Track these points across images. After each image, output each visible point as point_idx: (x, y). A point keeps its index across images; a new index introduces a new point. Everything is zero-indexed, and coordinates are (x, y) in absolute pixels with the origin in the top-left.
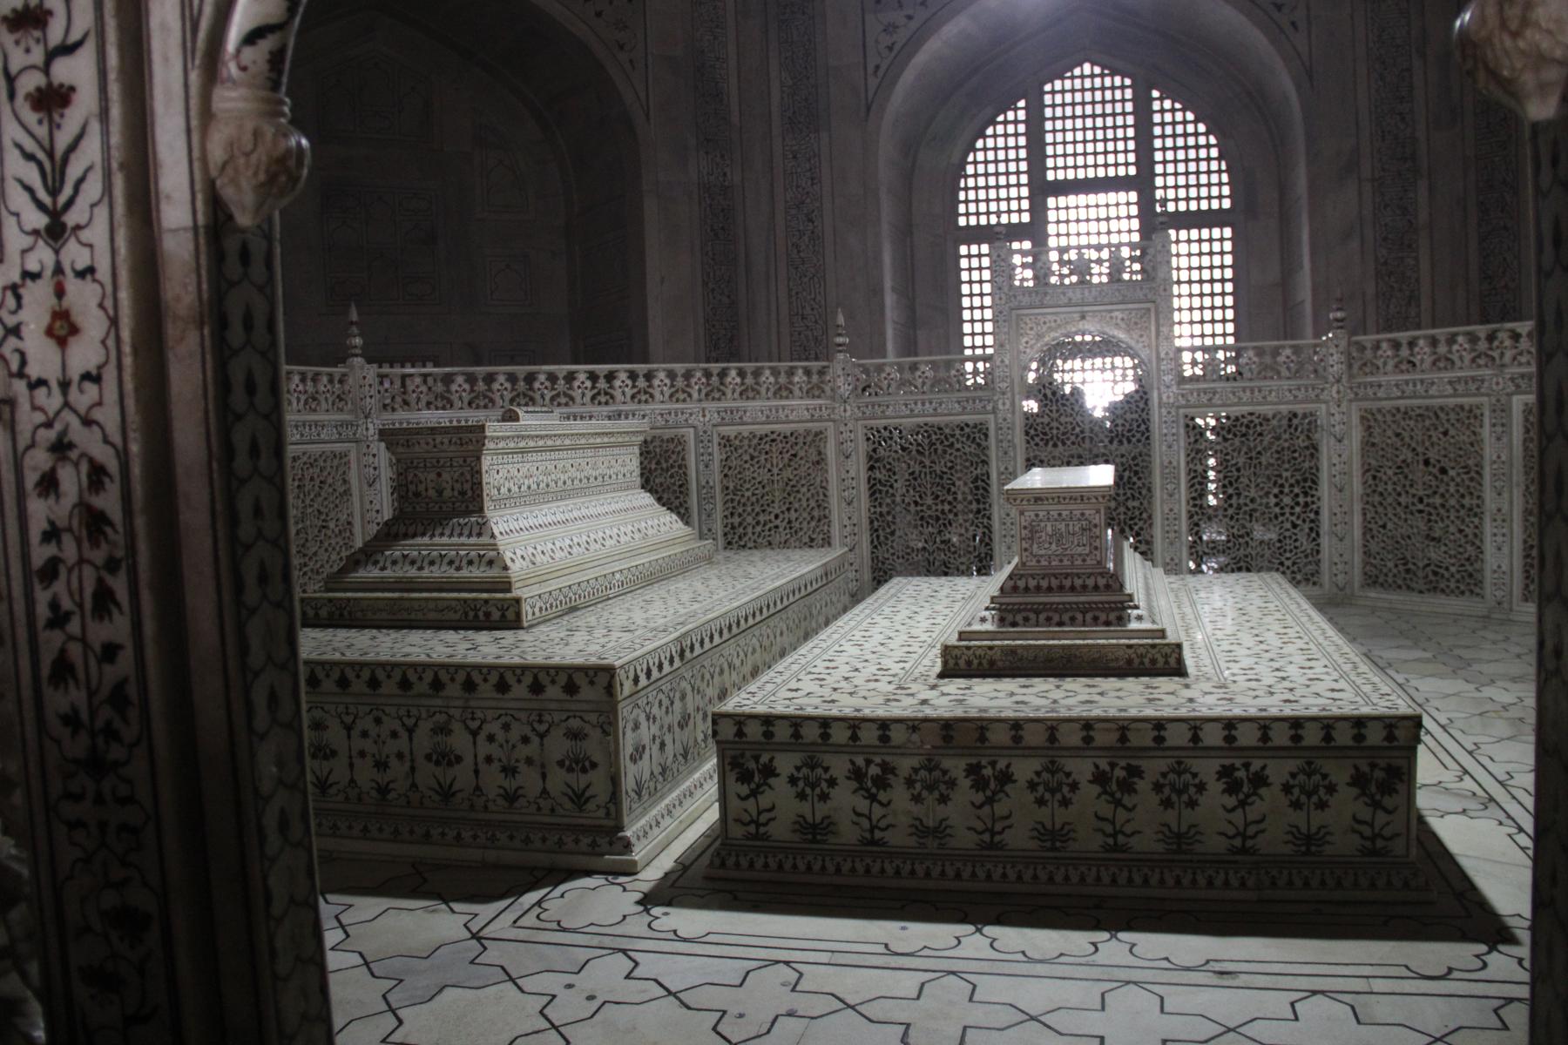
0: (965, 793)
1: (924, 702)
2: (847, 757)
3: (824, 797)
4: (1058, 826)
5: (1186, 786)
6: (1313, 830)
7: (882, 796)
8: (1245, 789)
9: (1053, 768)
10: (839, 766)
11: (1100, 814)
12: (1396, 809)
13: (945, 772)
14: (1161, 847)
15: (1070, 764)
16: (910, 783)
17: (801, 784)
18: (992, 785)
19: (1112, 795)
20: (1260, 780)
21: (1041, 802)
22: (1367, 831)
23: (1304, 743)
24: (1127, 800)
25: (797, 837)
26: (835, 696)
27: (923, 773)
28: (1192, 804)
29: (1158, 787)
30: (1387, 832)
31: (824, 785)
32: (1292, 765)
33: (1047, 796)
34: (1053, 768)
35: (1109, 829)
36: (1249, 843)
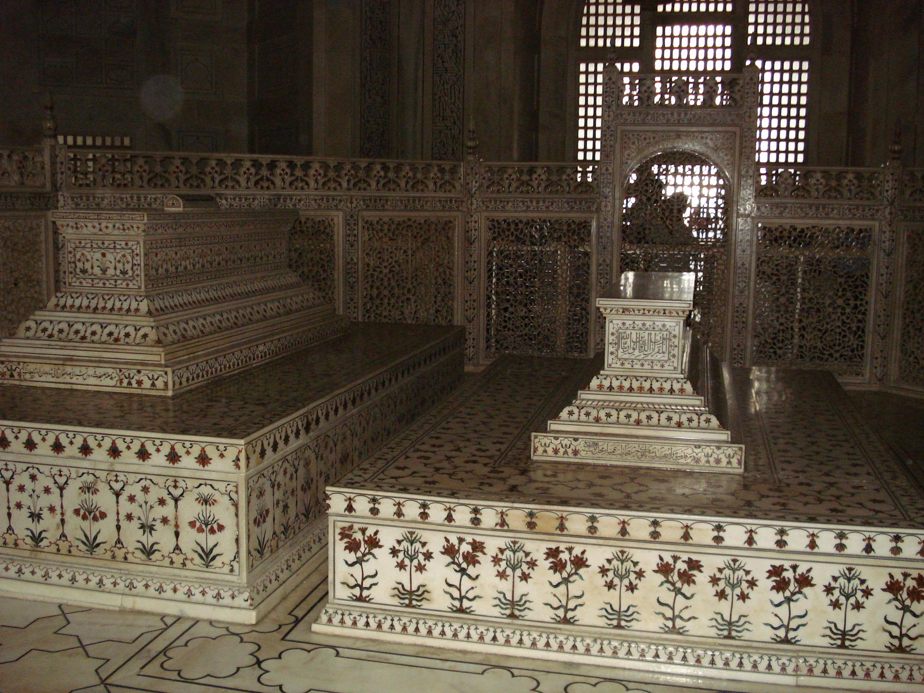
0: (543, 573)
2: (443, 535)
4: (624, 608)
5: (740, 582)
6: (848, 628)
15: (637, 555)
16: (496, 560)
17: (401, 555)
19: (673, 584)
20: (805, 581)
25: (396, 601)
29: (714, 581)
31: (421, 557)
33: (616, 581)
34: (622, 557)
35: (669, 614)
36: (791, 635)
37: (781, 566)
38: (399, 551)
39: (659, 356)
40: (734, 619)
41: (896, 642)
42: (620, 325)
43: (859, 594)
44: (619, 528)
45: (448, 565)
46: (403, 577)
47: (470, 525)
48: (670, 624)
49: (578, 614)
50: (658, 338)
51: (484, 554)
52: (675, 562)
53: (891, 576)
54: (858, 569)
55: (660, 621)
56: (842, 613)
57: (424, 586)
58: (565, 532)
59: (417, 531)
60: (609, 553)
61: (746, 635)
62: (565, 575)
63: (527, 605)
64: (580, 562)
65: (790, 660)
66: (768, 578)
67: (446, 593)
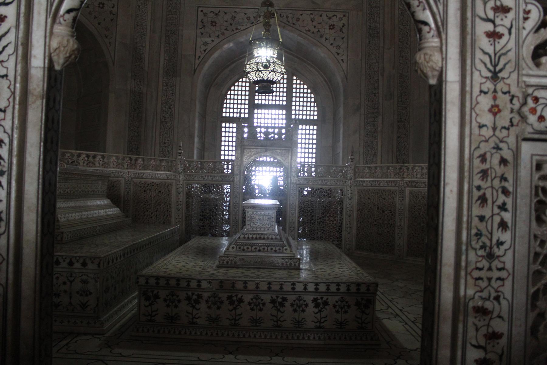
1: (213, 274)
3: (176, 306)
4: (258, 318)
7: (197, 306)
8: (321, 306)
13: (220, 298)
15: (263, 296)
16: (207, 302)
18: (236, 303)
19: (277, 307)
20: (326, 303)
23: (341, 291)
24: (282, 309)
26: (181, 271)
27: (212, 298)
28: (303, 311)
32: (337, 298)
33: (255, 307)
34: (257, 298)
35: (275, 319)
36: (322, 325)
60: (251, 296)
61: (305, 326)
62: (234, 306)
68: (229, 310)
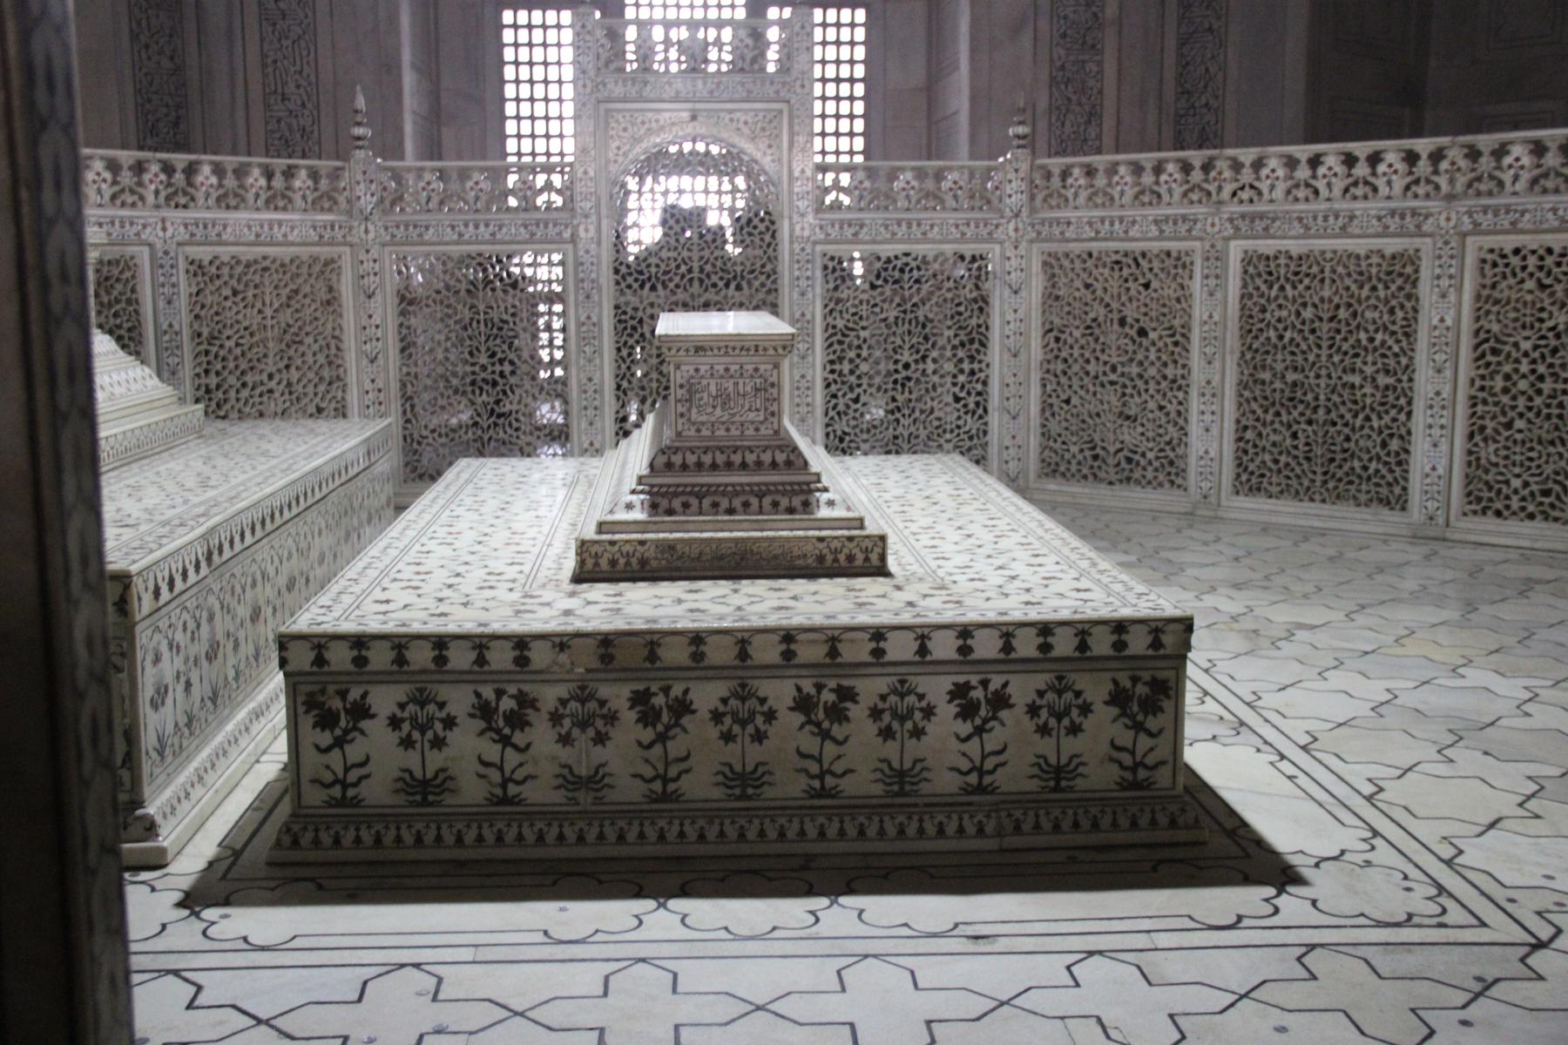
0: (629, 730)
1: (567, 613)
2: (471, 688)
3: (438, 743)
4: (749, 768)
5: (911, 711)
6: (1064, 761)
8: (983, 712)
9: (743, 693)
10: (459, 700)
11: (803, 749)
12: (1161, 731)
13: (602, 703)
14: (878, 789)
15: (765, 688)
16: (556, 718)
17: (406, 727)
18: (665, 717)
19: (818, 725)
20: (1000, 701)
21: (728, 737)
22: (1126, 759)
23: (1055, 653)
24: (837, 731)
25: (401, 799)
27: (573, 705)
28: (918, 733)
29: (876, 713)
30: (1150, 760)
31: (438, 726)
32: (1041, 680)
33: (736, 729)
34: (743, 693)
35: (814, 768)
36: (987, 780)
37: (967, 683)
38: (403, 720)
39: (752, 416)
40: (907, 765)
41: (1128, 775)
42: (692, 372)
43: (1075, 712)
44: (736, 650)
45: (481, 733)
46: (412, 759)
47: (513, 667)
48: (816, 784)
49: (684, 784)
50: (748, 389)
51: (538, 710)
52: (819, 692)
53: (1115, 682)
54: (1072, 676)
55: (803, 781)
56: (1053, 741)
57: (444, 770)
58: (658, 664)
59: (429, 686)
60: (720, 689)
61: (925, 788)
63: (606, 780)
64: (682, 707)
65: (988, 816)
66: (950, 702)
67: (480, 776)
68: (640, 744)
